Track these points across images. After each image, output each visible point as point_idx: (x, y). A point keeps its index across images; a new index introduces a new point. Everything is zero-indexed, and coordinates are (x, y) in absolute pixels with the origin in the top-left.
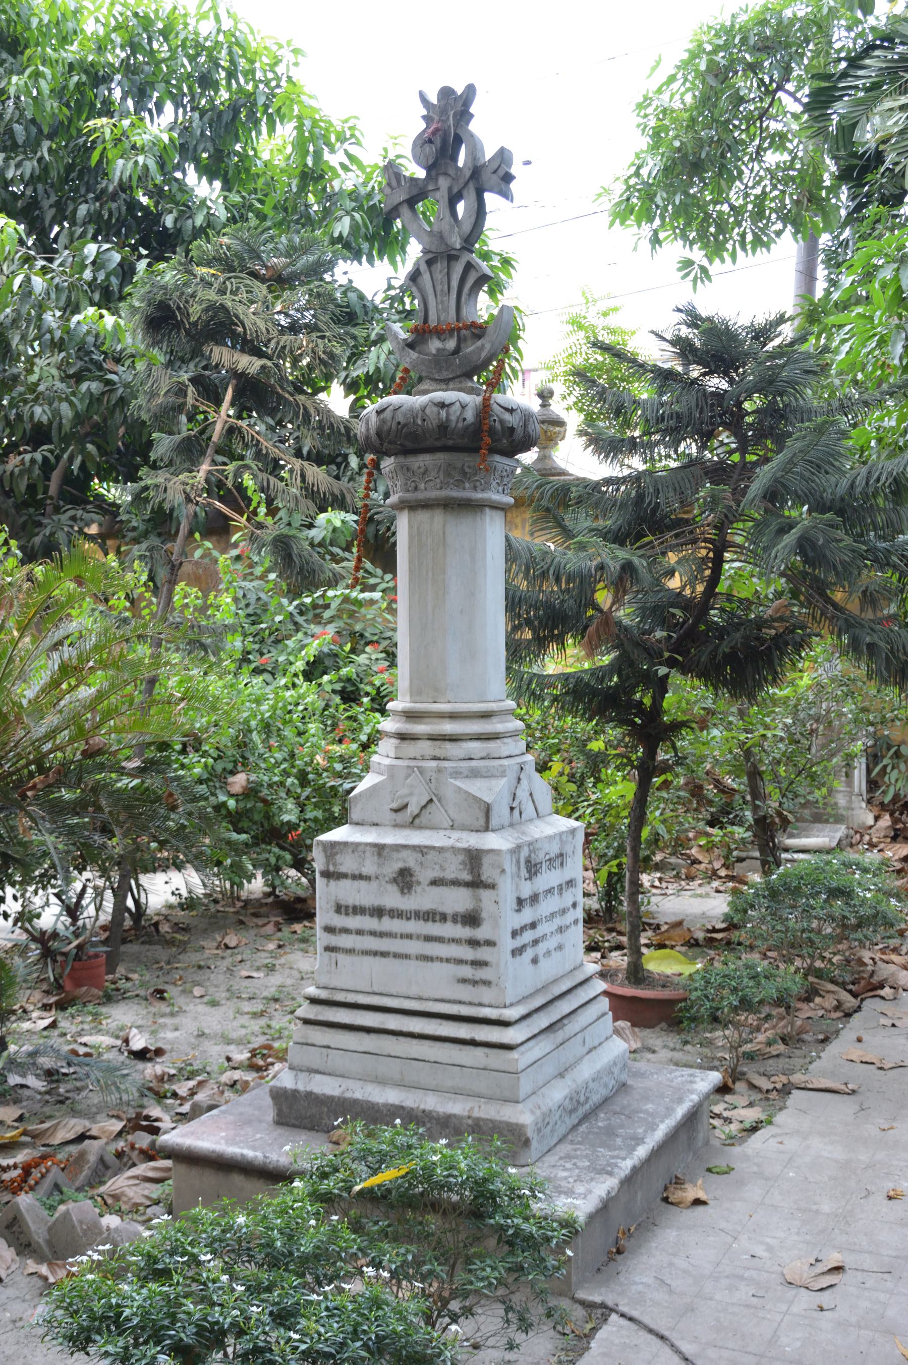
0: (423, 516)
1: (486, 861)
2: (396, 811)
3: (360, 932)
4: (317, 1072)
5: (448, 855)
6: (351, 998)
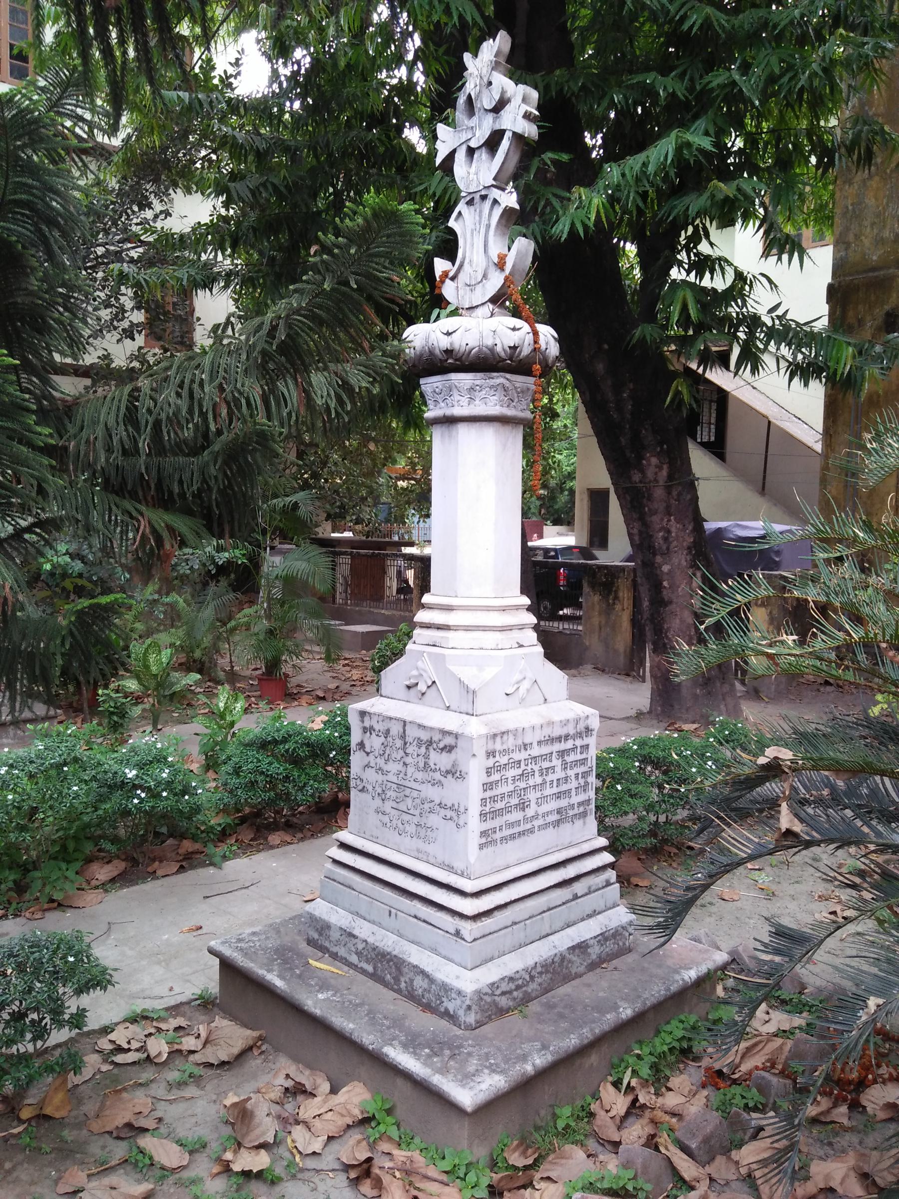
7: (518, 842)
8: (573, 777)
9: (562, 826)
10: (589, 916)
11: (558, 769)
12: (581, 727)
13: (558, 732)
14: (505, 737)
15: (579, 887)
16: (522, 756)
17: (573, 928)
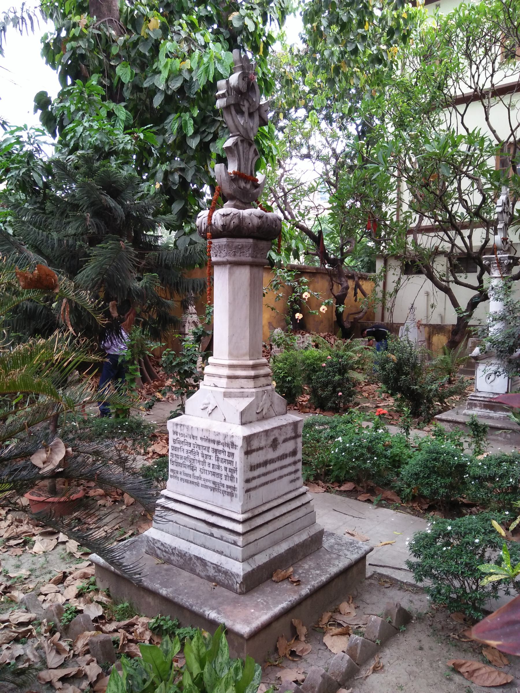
0: (256, 270)
3: (259, 476)
4: (254, 555)
6: (260, 510)
9: (216, 493)
10: (217, 552)
11: (213, 458)
12: (228, 440)
13: (212, 437)
15: (215, 531)
16: (192, 441)
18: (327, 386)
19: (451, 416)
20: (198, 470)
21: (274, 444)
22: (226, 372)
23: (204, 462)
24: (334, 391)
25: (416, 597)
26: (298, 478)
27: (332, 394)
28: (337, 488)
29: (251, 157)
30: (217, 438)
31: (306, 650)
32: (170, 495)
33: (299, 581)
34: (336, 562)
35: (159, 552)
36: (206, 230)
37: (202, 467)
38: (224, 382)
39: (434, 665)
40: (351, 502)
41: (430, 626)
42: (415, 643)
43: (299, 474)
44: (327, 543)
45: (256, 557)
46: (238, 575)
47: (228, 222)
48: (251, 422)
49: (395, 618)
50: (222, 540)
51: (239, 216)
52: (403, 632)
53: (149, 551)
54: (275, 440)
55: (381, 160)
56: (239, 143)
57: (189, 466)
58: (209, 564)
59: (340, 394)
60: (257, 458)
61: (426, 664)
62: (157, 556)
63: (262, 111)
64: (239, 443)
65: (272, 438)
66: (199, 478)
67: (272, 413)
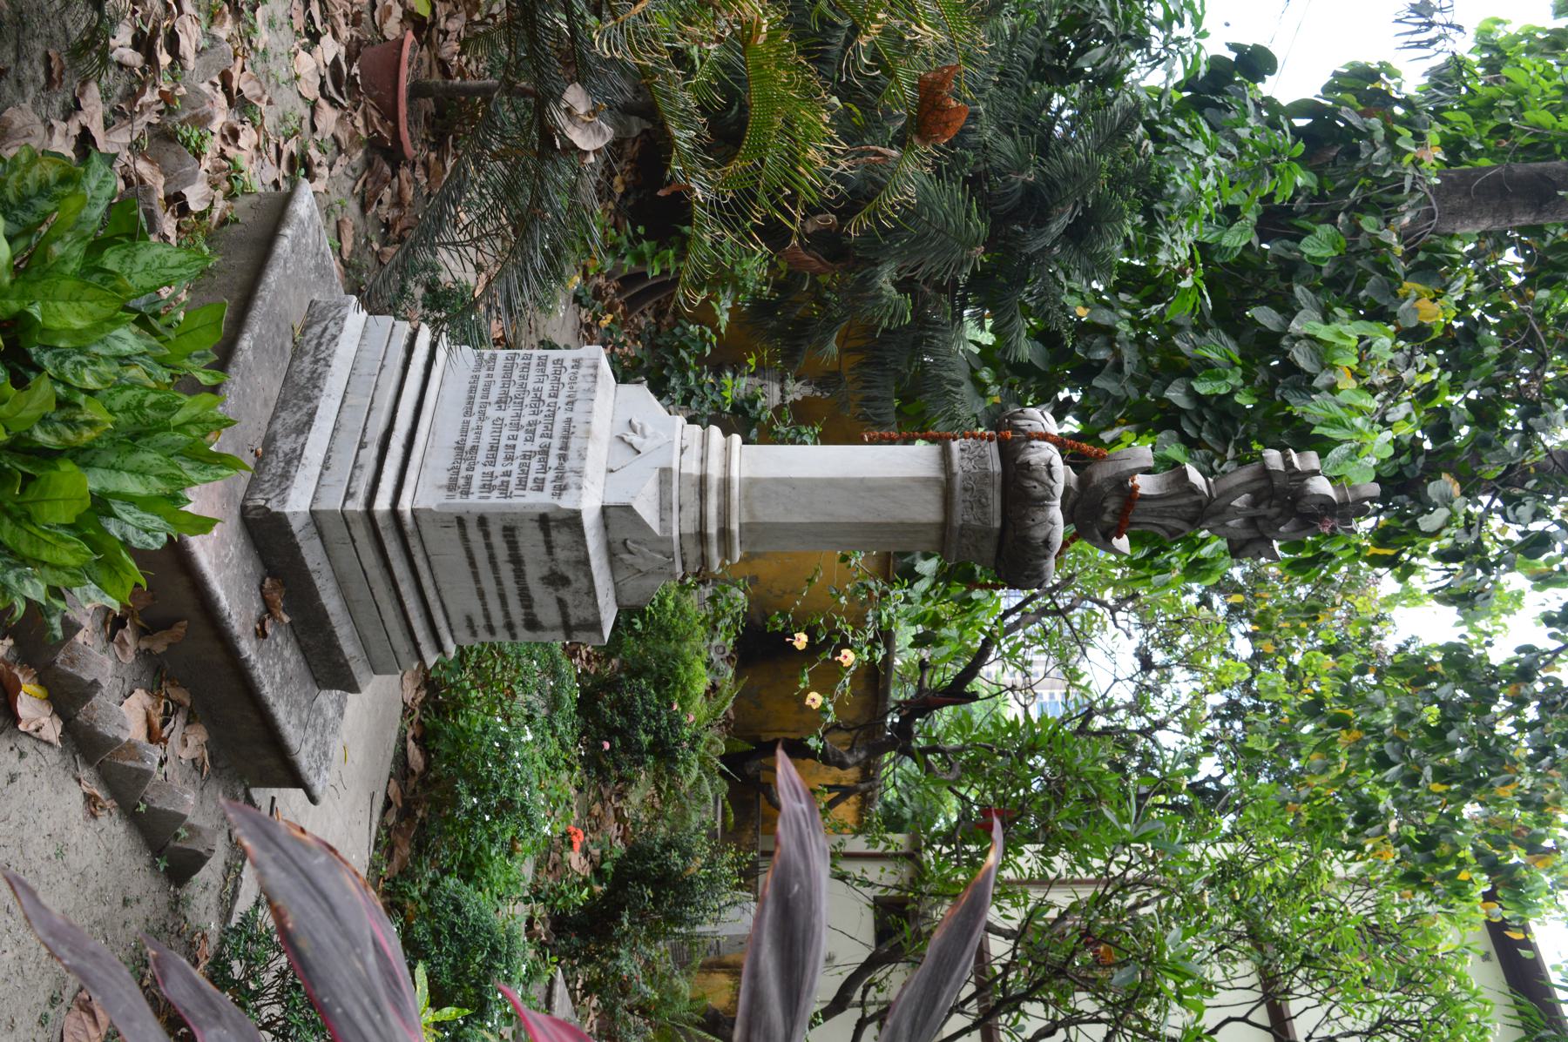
0: (934, 535)
1: (594, 636)
2: (624, 543)
3: (489, 546)
4: (322, 537)
5: (591, 610)
7: (464, 396)
8: (509, 468)
9: (453, 452)
10: (327, 458)
11: (529, 447)
12: (570, 479)
13: (574, 444)
14: (590, 379)
15: (372, 452)
16: (562, 400)
17: (330, 432)
18: (623, 713)
19: (562, 1006)
20: (501, 414)
21: (555, 580)
22: (715, 472)
23: (518, 427)
24: (611, 732)
25: (213, 900)
26: (474, 634)
27: (606, 727)
28: (411, 733)
29: (1167, 522)
30: (572, 454)
31: (123, 651)
32: (441, 354)
33: (265, 635)
34: (294, 720)
35: (317, 329)
36: (1017, 429)
37: (507, 421)
38: (693, 468)
39: (98, 929)
40: (387, 768)
41: (165, 925)
42: (135, 892)
43: (484, 636)
44: (327, 698)
45: (318, 541)
46: (284, 501)
47: (1036, 475)
48: (606, 527)
49: (188, 846)
50: (355, 467)
51: (1048, 498)
52: (154, 865)
53: (316, 310)
54: (564, 581)
55: (1145, 828)
56: (1195, 498)
57: (506, 394)
58: (301, 440)
59: (607, 746)
60: (531, 543)
61: (100, 911)
62: (307, 327)
63: (1259, 546)
64: (567, 502)
65: (571, 575)
66: (483, 416)
67: (622, 574)
